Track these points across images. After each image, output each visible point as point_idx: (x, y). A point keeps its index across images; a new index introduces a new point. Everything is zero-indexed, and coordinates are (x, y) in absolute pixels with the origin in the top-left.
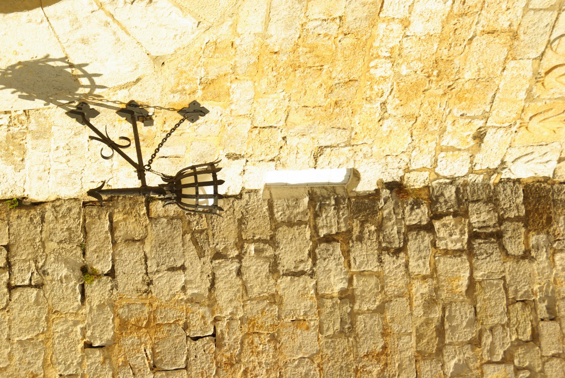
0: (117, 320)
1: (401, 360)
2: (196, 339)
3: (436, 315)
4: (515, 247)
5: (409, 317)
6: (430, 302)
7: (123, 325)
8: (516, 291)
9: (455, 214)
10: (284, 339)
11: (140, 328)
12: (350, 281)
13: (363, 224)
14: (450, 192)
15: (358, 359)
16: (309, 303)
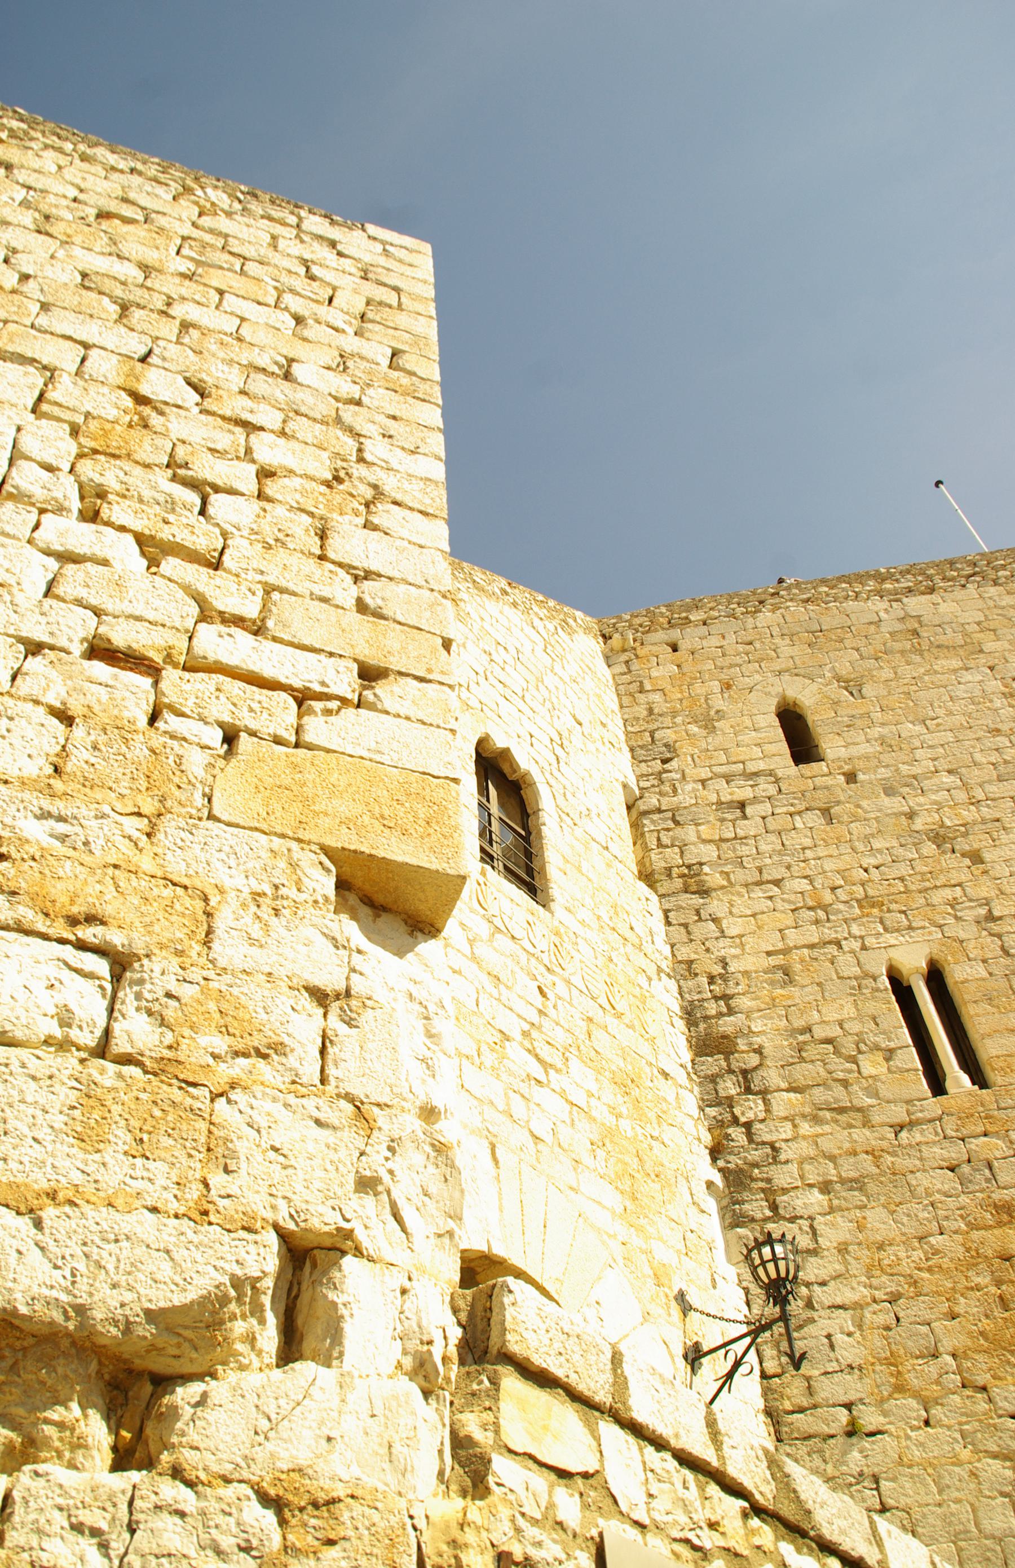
0: (896, 1395)
1: (875, 1139)
2: (898, 1320)
3: (828, 1115)
4: (754, 1060)
5: (835, 1137)
6: (816, 1120)
7: (900, 1388)
8: (792, 1057)
9: (731, 1107)
10: (879, 1238)
11: (899, 1372)
12: (811, 1186)
13: (753, 1179)
14: (712, 1112)
15: (883, 1174)
16: (839, 1219)
